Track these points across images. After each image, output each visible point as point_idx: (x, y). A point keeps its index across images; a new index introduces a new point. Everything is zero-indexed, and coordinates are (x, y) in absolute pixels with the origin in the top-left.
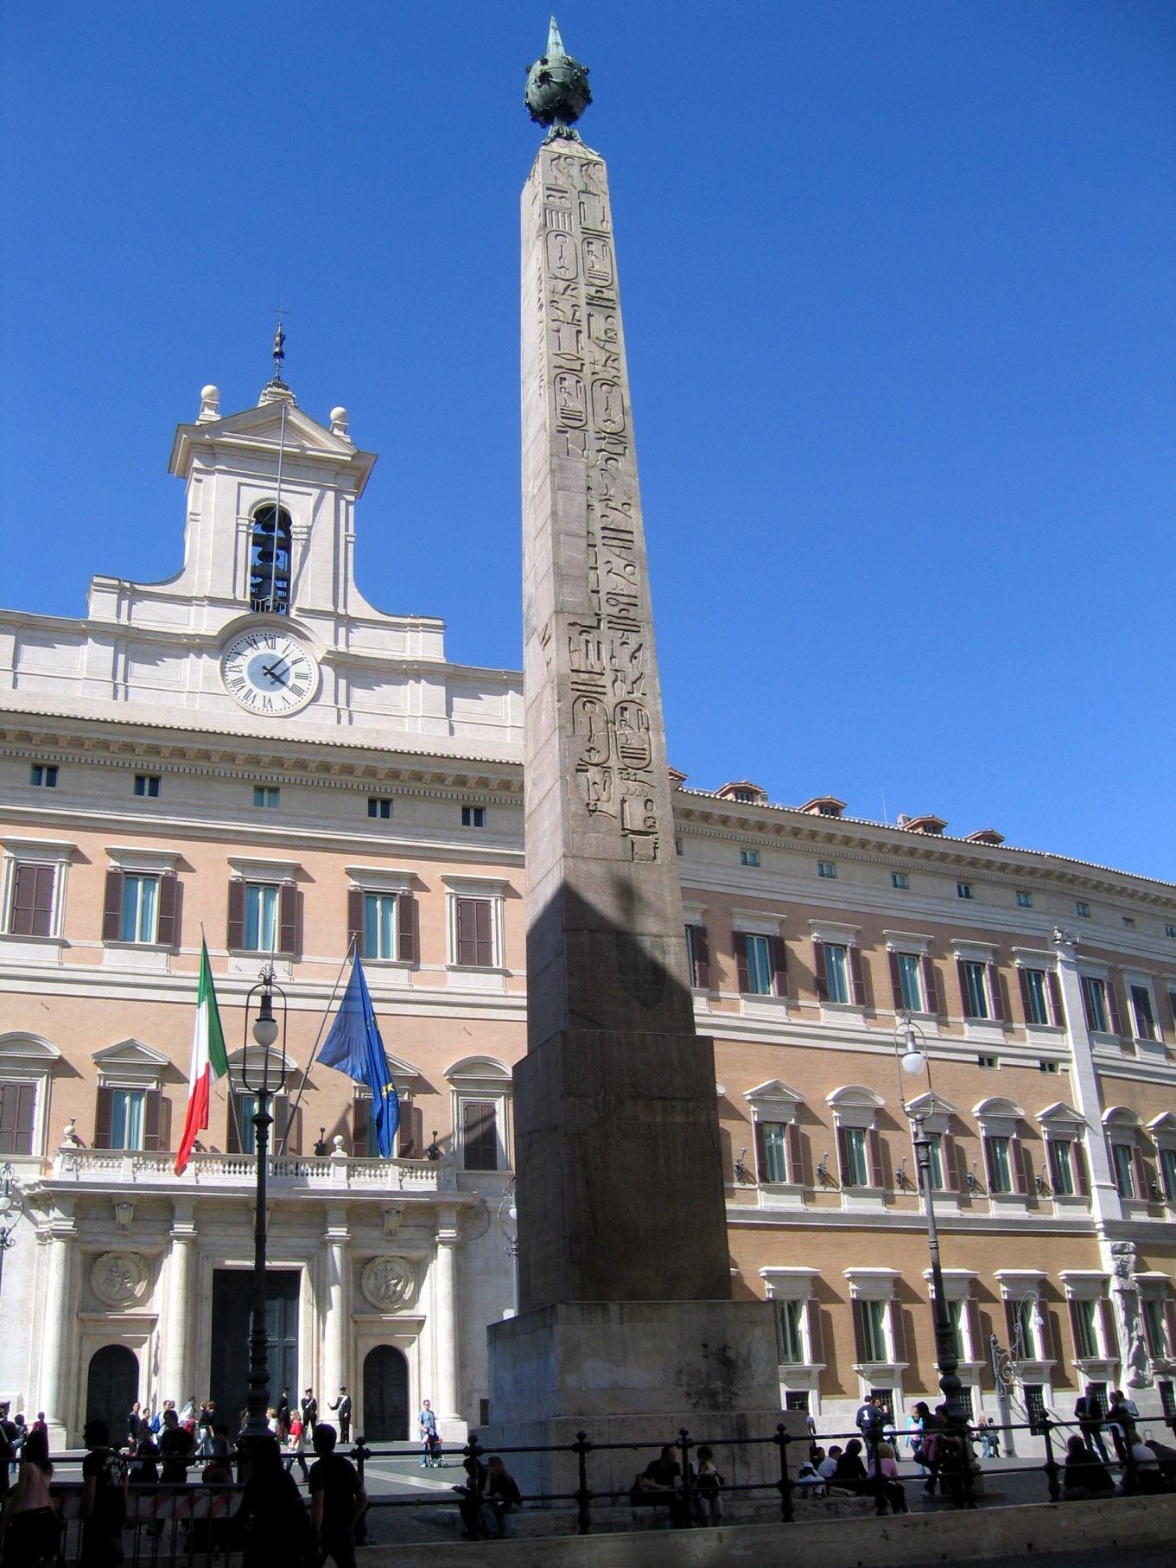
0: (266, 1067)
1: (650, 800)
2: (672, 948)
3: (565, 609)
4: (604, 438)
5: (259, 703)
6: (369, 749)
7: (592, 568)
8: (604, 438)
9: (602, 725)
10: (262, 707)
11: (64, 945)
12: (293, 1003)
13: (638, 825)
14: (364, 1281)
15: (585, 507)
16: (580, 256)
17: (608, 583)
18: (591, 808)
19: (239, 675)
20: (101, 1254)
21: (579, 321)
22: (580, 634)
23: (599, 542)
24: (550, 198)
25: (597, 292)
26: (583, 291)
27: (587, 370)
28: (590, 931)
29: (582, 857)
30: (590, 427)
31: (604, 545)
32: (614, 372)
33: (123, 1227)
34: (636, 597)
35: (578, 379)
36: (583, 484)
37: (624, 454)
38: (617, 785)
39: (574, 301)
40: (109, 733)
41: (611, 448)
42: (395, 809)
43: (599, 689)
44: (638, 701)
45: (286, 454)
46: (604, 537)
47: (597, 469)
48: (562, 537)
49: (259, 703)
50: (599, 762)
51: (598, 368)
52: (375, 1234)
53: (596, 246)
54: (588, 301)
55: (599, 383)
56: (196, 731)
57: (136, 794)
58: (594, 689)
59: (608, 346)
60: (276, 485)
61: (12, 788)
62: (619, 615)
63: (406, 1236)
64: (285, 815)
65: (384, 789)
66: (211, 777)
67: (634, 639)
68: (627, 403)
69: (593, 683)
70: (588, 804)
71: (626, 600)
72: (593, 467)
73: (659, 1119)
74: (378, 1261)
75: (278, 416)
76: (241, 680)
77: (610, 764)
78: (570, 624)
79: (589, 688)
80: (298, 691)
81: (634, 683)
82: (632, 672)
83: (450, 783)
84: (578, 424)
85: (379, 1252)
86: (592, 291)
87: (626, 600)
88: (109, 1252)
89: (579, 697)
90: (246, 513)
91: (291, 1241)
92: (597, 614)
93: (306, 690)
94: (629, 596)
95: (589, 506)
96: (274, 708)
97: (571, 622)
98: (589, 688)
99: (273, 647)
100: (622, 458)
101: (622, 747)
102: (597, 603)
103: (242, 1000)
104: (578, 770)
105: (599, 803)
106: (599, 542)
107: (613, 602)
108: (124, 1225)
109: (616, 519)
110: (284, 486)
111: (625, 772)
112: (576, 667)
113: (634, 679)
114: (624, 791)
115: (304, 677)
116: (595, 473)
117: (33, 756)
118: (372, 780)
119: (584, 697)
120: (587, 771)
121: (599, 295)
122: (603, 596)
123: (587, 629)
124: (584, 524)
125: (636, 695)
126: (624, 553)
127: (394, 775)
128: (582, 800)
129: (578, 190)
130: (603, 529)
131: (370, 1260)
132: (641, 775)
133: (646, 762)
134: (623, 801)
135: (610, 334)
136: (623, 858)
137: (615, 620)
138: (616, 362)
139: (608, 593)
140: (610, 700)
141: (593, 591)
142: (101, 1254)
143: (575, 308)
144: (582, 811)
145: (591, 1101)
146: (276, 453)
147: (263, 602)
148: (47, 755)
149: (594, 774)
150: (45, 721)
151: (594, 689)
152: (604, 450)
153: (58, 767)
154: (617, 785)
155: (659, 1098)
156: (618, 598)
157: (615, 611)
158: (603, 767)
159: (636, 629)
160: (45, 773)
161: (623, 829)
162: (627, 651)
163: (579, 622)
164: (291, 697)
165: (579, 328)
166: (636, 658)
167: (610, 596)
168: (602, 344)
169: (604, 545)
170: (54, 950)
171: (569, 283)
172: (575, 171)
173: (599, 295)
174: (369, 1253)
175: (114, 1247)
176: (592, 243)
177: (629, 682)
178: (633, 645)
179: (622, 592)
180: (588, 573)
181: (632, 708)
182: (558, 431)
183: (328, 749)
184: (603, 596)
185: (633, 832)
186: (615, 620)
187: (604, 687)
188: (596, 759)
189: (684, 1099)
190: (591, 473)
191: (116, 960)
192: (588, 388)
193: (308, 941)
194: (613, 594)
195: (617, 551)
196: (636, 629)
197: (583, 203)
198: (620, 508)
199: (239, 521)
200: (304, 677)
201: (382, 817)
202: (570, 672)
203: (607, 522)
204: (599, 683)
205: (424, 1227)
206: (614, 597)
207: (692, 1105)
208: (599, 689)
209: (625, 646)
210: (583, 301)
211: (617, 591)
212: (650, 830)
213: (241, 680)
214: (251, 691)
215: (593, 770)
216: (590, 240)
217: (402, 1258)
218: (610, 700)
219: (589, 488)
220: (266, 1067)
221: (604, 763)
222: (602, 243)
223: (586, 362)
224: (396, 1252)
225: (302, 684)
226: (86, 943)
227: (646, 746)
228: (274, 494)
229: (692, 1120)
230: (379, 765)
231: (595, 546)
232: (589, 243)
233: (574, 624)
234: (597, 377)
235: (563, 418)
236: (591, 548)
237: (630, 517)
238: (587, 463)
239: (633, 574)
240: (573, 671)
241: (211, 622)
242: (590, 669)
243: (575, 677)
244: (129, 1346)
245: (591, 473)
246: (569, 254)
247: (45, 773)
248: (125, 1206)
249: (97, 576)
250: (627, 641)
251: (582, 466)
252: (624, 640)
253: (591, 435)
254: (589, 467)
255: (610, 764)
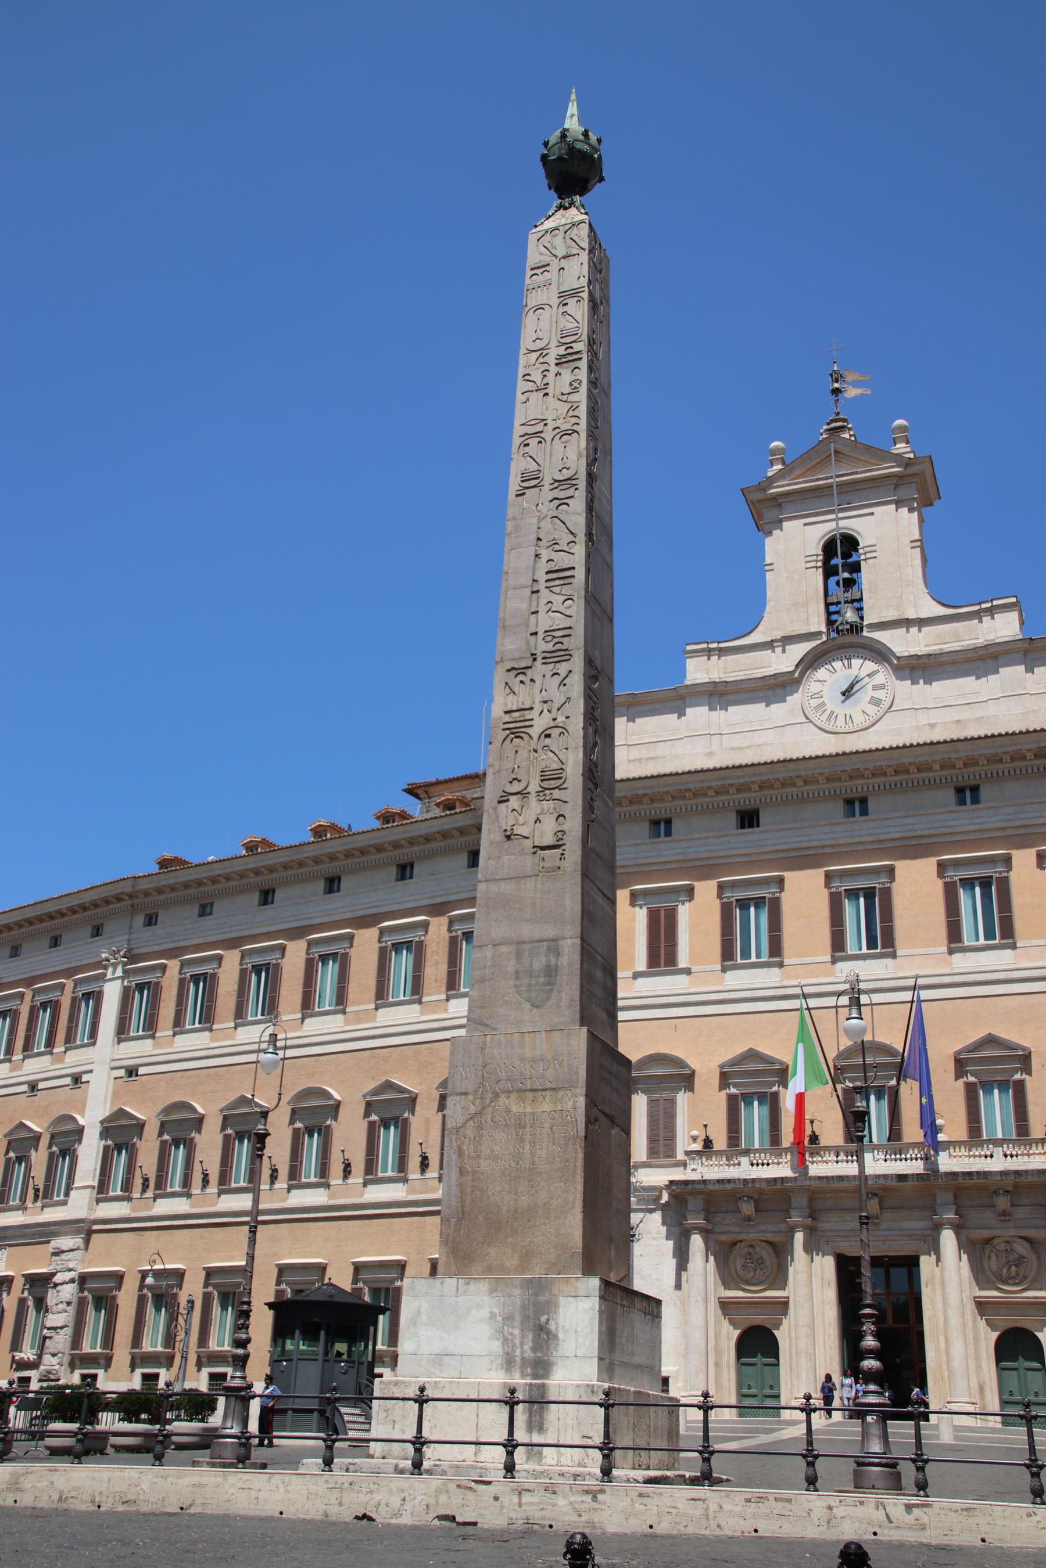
0: (864, 1061)
1: (562, 815)
2: (566, 950)
3: (505, 658)
4: (556, 488)
5: (841, 721)
6: (938, 743)
7: (533, 613)
8: (556, 488)
9: (526, 755)
10: (843, 725)
11: (688, 971)
12: (877, 998)
13: (549, 840)
14: (985, 1262)
15: (533, 557)
16: (554, 320)
17: (544, 622)
18: (508, 833)
19: (820, 701)
20: (735, 1244)
21: (547, 384)
22: (516, 676)
23: (542, 586)
24: (534, 277)
25: (566, 349)
26: (555, 352)
27: (551, 425)
28: (494, 945)
29: (495, 880)
30: (547, 481)
31: (547, 587)
32: (574, 420)
33: (749, 1219)
34: (570, 628)
35: (540, 439)
36: (534, 537)
37: (572, 497)
38: (534, 807)
39: (545, 367)
40: (702, 781)
41: (562, 495)
42: (984, 793)
43: (527, 723)
44: (561, 725)
45: (840, 485)
46: (547, 581)
47: (548, 519)
48: (509, 593)
49: (841, 721)
50: (519, 789)
51: (558, 423)
52: (989, 1214)
53: (572, 302)
54: (557, 361)
55: (558, 436)
56: (887, 749)
57: (737, 828)
58: (522, 724)
59: (572, 398)
60: (833, 516)
61: (635, 845)
62: (554, 649)
63: (1021, 1216)
64: (873, 820)
65: (968, 777)
66: (802, 800)
67: (563, 668)
68: (583, 444)
69: (522, 719)
70: (506, 830)
71: (561, 633)
72: (544, 518)
73: (529, 1110)
74: (996, 1241)
75: (827, 454)
76: (823, 704)
77: (528, 790)
78: (508, 671)
79: (518, 725)
80: (876, 702)
81: (558, 709)
82: (558, 698)
83: (1033, 757)
84: (537, 481)
85: (995, 1232)
86: (562, 351)
87: (561, 633)
88: (741, 1241)
89: (508, 735)
90: (816, 549)
91: (906, 1224)
92: (533, 655)
93: (884, 699)
94: (565, 629)
95: (537, 556)
96: (855, 725)
97: (509, 668)
98: (518, 725)
99: (850, 666)
100: (572, 499)
101: (542, 772)
102: (533, 643)
103: (831, 1001)
104: (500, 802)
105: (515, 827)
106: (542, 586)
107: (549, 639)
108: (749, 1216)
109: (562, 560)
110: (841, 515)
111: (542, 794)
112: (509, 708)
113: (559, 706)
114: (539, 811)
115: (882, 687)
116: (546, 524)
117: (648, 814)
118: (953, 771)
119: (512, 733)
120: (508, 800)
121: (569, 351)
122: (541, 635)
123: (522, 671)
124: (531, 574)
125: (561, 719)
126: (566, 590)
127: (970, 762)
128: (501, 827)
129: (560, 256)
130: (547, 573)
131: (988, 1241)
132: (557, 794)
133: (563, 780)
134: (538, 820)
135: (575, 384)
136: (531, 873)
137: (548, 655)
138: (577, 410)
139: (546, 632)
140: (535, 732)
141: (532, 634)
142: (735, 1244)
143: (545, 373)
144: (499, 837)
145: (471, 1097)
146: (830, 487)
147: (837, 627)
148: (659, 810)
149: (514, 802)
150: (647, 781)
151: (522, 724)
152: (556, 499)
153: (979, 785)
154: (534, 807)
155: (532, 1090)
156: (556, 634)
157: (550, 647)
158: (523, 794)
159: (567, 657)
160: (662, 826)
161: (534, 847)
162: (557, 680)
163: (516, 666)
164: (871, 710)
165: (545, 391)
166: (565, 685)
167: (546, 634)
168: (564, 398)
169: (547, 587)
170: (683, 978)
171: (540, 352)
172: (558, 241)
173: (569, 351)
174: (985, 1233)
175: (744, 1236)
176: (567, 304)
177: (554, 710)
178: (563, 674)
179: (558, 627)
180: (529, 619)
181: (555, 732)
182: (517, 496)
183: (898, 751)
184: (541, 635)
185: (543, 848)
186: (548, 655)
187: (532, 720)
188: (516, 787)
189: (554, 1089)
190: (542, 524)
191: (738, 980)
192: (549, 443)
193: (1018, 925)
194: (550, 631)
195: (557, 590)
196: (567, 657)
197: (563, 268)
198: (565, 548)
199: (808, 559)
200: (882, 687)
201: (861, 815)
202: (502, 714)
203: (552, 566)
204: (528, 717)
205: (1041, 1205)
206: (550, 633)
207: (561, 1093)
208: (527, 723)
209: (555, 676)
210: (552, 361)
211: (553, 628)
212: (560, 843)
213: (823, 704)
214: (832, 712)
215: (512, 798)
216: (565, 302)
217: (1021, 1237)
218: (535, 732)
219: (539, 539)
220: (864, 1061)
221: (526, 788)
222: (576, 299)
223: (549, 422)
224: (1013, 1232)
225: (880, 694)
226: (708, 967)
227: (564, 767)
228: (832, 525)
229: (559, 1108)
230: (953, 756)
231: (538, 591)
232: (564, 305)
233: (513, 669)
234: (558, 431)
235: (522, 481)
236: (534, 595)
237: (573, 554)
238: (539, 516)
239: (569, 607)
240: (506, 712)
241: (784, 661)
242: (521, 706)
243: (507, 718)
244: (768, 1326)
245: (542, 524)
246: (544, 324)
247: (662, 826)
248: (745, 1198)
249: (687, 644)
250: (558, 671)
251: (535, 521)
252: (555, 671)
253: (547, 487)
254: (539, 521)
255: (529, 790)
